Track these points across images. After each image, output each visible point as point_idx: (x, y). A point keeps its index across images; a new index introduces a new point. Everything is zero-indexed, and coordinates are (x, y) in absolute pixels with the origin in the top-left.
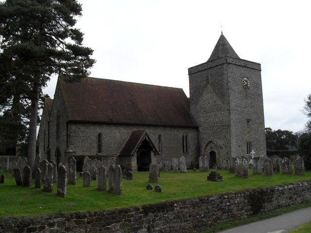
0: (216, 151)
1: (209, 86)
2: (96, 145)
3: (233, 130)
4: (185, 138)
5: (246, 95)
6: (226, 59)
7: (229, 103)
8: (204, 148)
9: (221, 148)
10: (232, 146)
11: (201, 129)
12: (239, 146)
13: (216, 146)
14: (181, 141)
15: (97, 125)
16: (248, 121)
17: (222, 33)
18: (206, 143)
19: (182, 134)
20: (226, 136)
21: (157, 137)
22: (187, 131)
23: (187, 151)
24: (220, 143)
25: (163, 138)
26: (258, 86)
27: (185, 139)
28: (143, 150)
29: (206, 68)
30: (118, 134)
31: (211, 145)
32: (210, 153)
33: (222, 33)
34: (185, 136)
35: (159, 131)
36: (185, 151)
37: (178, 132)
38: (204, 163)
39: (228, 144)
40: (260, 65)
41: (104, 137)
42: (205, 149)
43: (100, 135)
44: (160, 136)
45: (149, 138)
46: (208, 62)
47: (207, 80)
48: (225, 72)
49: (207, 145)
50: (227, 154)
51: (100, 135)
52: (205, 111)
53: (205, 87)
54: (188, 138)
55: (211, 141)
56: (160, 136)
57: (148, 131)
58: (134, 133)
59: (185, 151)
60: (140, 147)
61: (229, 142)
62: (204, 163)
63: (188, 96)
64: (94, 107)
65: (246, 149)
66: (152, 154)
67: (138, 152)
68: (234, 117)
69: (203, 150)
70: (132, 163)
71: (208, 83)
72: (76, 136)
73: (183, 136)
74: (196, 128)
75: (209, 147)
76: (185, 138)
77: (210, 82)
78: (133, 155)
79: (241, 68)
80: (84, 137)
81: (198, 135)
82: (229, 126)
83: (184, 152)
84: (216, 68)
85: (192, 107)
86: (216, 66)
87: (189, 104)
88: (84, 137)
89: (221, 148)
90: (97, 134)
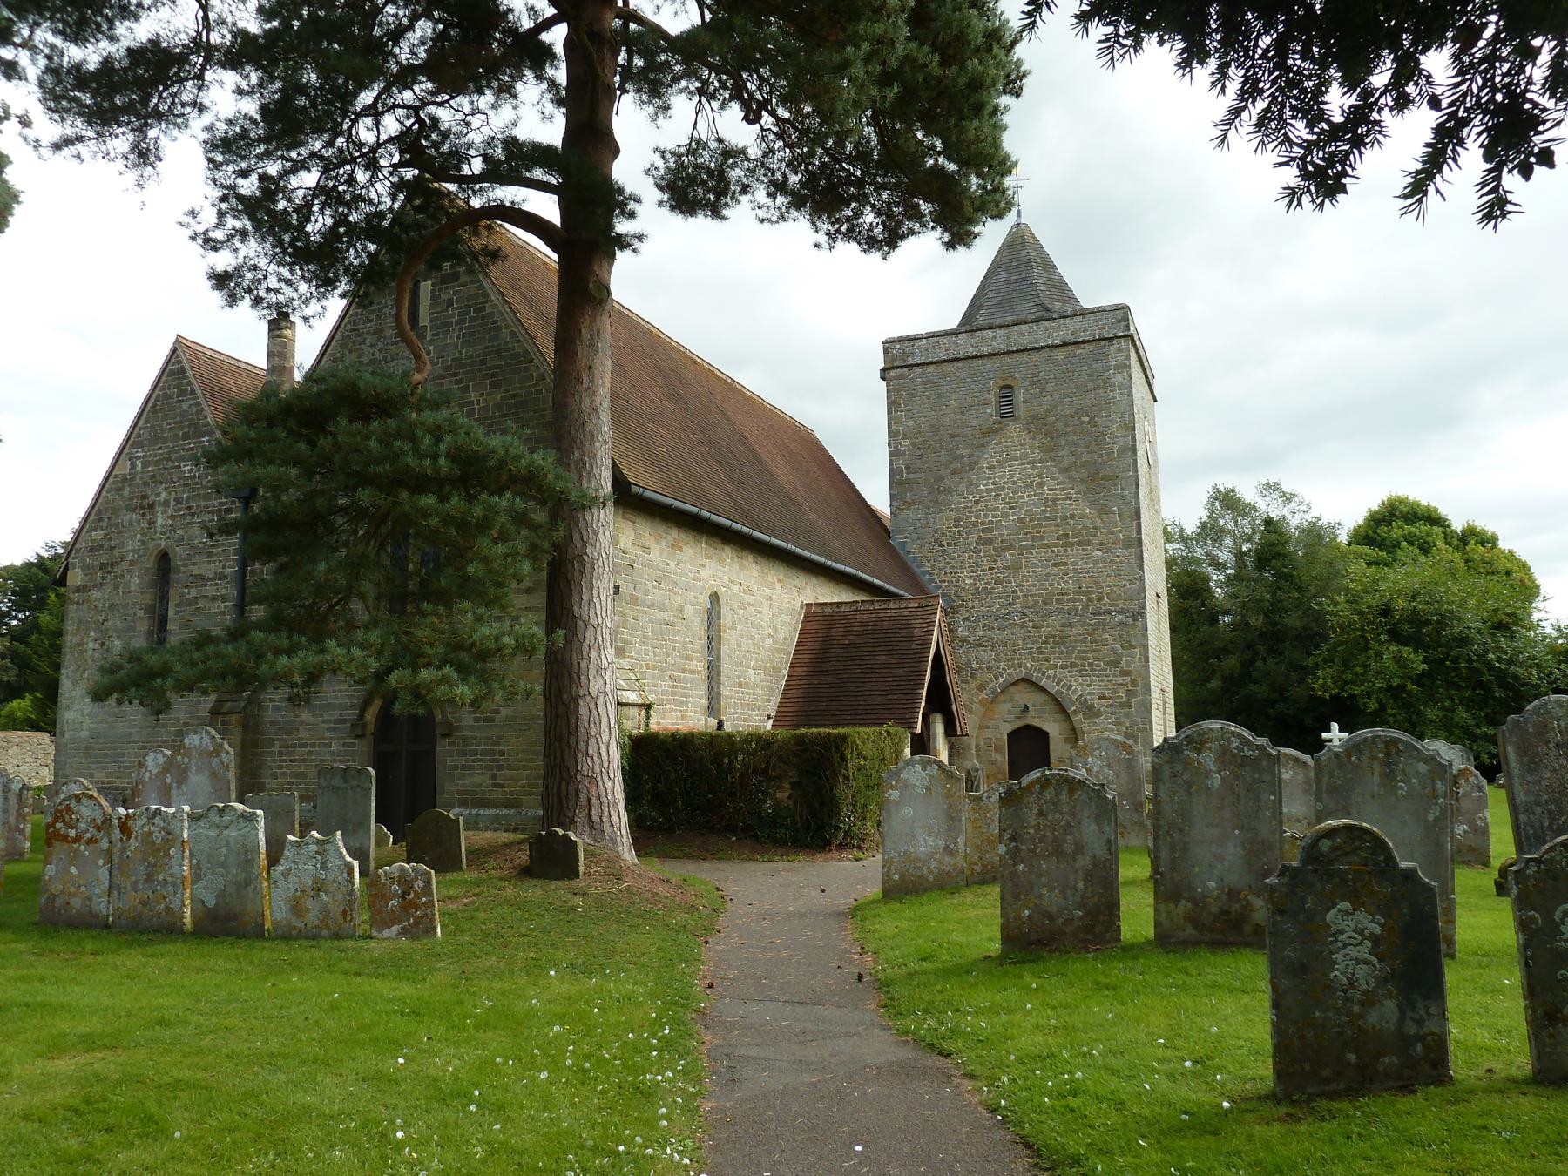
1: (1012, 425)
20: (1119, 657)
24: (1077, 687)
31: (1023, 696)
39: (1130, 693)
53: (990, 433)
75: (1004, 708)
77: (1021, 410)
84: (1060, 355)
86: (1065, 344)
89: (1091, 712)
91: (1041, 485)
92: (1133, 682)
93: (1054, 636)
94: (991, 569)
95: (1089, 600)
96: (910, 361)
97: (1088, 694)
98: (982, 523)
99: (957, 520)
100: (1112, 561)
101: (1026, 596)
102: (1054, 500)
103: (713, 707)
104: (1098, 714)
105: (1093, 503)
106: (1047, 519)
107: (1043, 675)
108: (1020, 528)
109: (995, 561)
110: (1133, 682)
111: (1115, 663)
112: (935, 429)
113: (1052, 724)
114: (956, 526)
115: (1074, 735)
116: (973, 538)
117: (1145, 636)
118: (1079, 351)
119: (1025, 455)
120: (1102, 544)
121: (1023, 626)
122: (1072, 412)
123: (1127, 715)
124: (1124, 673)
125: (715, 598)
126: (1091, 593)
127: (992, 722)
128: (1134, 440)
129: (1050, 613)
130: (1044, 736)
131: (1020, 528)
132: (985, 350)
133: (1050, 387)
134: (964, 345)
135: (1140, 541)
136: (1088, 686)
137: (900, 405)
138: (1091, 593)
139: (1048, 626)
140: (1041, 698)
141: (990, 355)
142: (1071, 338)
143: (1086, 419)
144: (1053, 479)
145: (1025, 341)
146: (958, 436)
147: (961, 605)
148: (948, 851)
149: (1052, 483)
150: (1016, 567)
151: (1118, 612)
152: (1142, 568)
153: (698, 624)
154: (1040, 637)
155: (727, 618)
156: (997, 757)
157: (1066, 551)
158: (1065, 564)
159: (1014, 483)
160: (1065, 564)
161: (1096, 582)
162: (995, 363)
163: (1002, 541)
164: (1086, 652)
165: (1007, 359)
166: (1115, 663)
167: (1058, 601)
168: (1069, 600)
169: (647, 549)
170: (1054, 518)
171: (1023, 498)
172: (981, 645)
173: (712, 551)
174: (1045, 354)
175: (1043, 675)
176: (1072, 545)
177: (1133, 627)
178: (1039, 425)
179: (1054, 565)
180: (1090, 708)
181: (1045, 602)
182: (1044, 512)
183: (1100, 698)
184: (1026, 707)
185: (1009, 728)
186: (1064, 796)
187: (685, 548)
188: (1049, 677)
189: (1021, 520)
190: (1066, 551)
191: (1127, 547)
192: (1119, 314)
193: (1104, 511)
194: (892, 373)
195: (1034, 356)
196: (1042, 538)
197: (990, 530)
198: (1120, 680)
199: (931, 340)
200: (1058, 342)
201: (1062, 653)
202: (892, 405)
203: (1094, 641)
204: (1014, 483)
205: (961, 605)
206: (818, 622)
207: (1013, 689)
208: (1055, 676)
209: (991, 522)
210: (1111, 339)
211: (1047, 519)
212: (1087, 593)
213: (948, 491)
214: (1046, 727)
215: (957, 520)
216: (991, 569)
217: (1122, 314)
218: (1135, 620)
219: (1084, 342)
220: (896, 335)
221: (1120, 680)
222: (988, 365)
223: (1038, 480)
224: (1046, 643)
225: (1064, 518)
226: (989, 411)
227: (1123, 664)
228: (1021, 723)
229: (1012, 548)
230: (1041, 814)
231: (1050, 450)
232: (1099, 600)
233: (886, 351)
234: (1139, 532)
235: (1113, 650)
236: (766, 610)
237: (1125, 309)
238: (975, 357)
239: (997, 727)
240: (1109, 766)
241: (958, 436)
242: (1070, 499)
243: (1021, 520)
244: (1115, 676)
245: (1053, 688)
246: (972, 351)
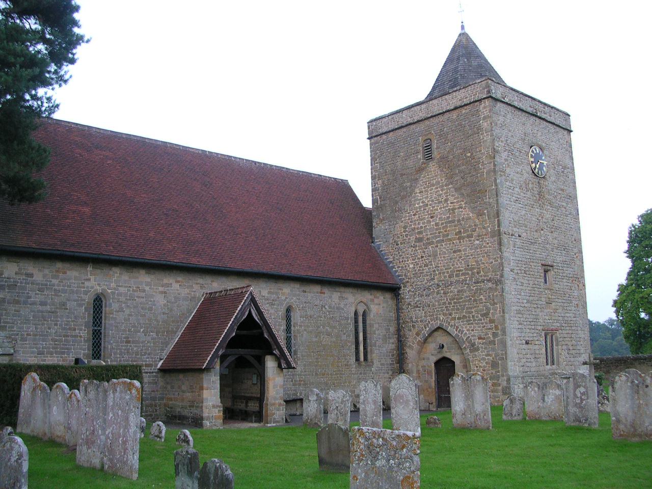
1: (431, 164)
2: (85, 333)
3: (510, 287)
4: (360, 319)
5: (540, 193)
6: (488, 86)
7: (498, 214)
8: (415, 346)
9: (474, 348)
10: (509, 343)
11: (405, 292)
12: (527, 343)
13: (457, 342)
14: (352, 327)
15: (90, 268)
16: (547, 269)
17: (463, 27)
18: (426, 332)
19: (354, 310)
20: (488, 309)
21: (282, 312)
22: (366, 296)
23: (366, 359)
24: (468, 331)
25: (296, 317)
26: (567, 171)
27: (361, 320)
28: (242, 351)
29: (422, 115)
30: (161, 300)
31: (440, 338)
32: (437, 363)
33: (463, 27)
34: (361, 312)
35: (288, 293)
36: (362, 358)
37: (341, 298)
38: (469, 396)
39: (495, 335)
40: (569, 116)
41: (111, 308)
42: (419, 352)
43: (98, 304)
44: (288, 310)
45: (260, 313)
46: (431, 97)
48: (485, 125)
49: (426, 340)
50: (494, 365)
51: (98, 304)
53: (420, 170)
54: (371, 317)
55: (439, 328)
56: (288, 310)
57: (262, 291)
58: (211, 300)
59: (362, 358)
60: (233, 343)
61: (499, 329)
62: (469, 396)
63: (367, 201)
64: (87, 210)
65: (544, 350)
66: (270, 364)
67: (223, 358)
68: (512, 254)
69: (411, 354)
70: (206, 394)
72: (18, 302)
73: (356, 313)
74: (393, 290)
75: (432, 347)
76: (360, 319)
77: (435, 154)
78: (208, 369)
79: (523, 117)
80: (43, 304)
81: (398, 310)
82: (499, 282)
83: (357, 359)
84: (454, 115)
85: (379, 229)
86: (456, 108)
87: (372, 223)
88: (43, 304)
89: (474, 348)
90: (88, 299)
91: (446, 200)
92: (496, 327)
93: (454, 299)
94: (422, 257)
95: (473, 274)
96: (381, 131)
97: (472, 336)
98: (418, 228)
99: (405, 227)
100: (484, 247)
101: (440, 273)
102: (453, 209)
104: (477, 349)
105: (473, 209)
106: (450, 222)
107: (449, 324)
108: (437, 229)
109: (424, 252)
110: (496, 327)
111: (486, 315)
112: (393, 173)
113: (456, 356)
114: (404, 232)
116: (413, 238)
118: (464, 112)
119: (438, 183)
120: (479, 236)
121: (438, 293)
122: (461, 151)
123: (493, 349)
124: (491, 321)
126: (474, 269)
127: (426, 356)
129: (451, 284)
130: (453, 363)
131: (437, 229)
136: (473, 330)
137: (376, 160)
138: (474, 269)
139: (451, 292)
140: (450, 339)
142: (459, 104)
143: (469, 154)
144: (453, 196)
145: (436, 110)
146: (404, 174)
147: (408, 282)
149: (451, 199)
150: (435, 256)
151: (488, 281)
154: (447, 300)
157: (460, 242)
158: (460, 251)
159: (433, 201)
160: (460, 251)
161: (477, 262)
163: (428, 239)
164: (471, 308)
165: (427, 122)
166: (486, 315)
167: (457, 275)
168: (463, 274)
169: (31, 275)
170: (453, 221)
171: (437, 210)
172: (417, 307)
174: (447, 116)
175: (449, 324)
177: (496, 290)
178: (444, 161)
179: (455, 252)
180: (473, 345)
181: (450, 277)
182: (448, 218)
183: (479, 338)
184: (443, 346)
185: (434, 359)
187: (69, 273)
188: (452, 326)
189: (437, 224)
190: (460, 242)
191: (493, 237)
193: (480, 214)
195: (441, 118)
196: (448, 235)
198: (489, 326)
199: (390, 117)
200: (452, 108)
201: (458, 309)
203: (475, 300)
204: (433, 201)
205: (408, 282)
207: (436, 334)
208: (455, 325)
209: (422, 227)
210: (480, 101)
211: (450, 222)
212: (472, 269)
213: (400, 210)
215: (405, 227)
216: (422, 257)
219: (465, 105)
221: (489, 326)
223: (445, 198)
224: (450, 303)
225: (459, 221)
226: (419, 157)
227: (490, 315)
228: (440, 356)
229: (432, 243)
231: (450, 178)
232: (478, 273)
233: (369, 128)
235: (485, 306)
238: (410, 124)
239: (428, 359)
241: (404, 174)
242: (461, 208)
243: (437, 224)
244: (486, 323)
245: (454, 332)
246: (410, 120)
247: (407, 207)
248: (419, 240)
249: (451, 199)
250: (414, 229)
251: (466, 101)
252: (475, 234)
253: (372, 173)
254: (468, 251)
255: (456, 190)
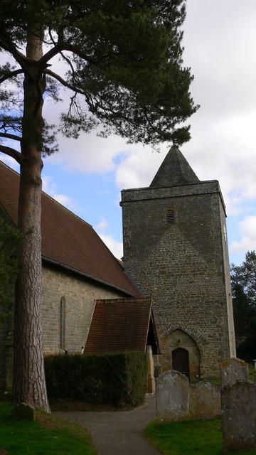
0: (190, 350)
1: (174, 228)
13: (192, 340)
24: (200, 333)
31: (178, 336)
47: (171, 219)
50: (220, 353)
52: (163, 273)
53: (164, 229)
71: (171, 219)
77: (177, 220)
84: (192, 199)
86: (194, 195)
89: (205, 342)
92: (222, 330)
99: (151, 264)
103: (62, 346)
110: (222, 330)
111: (215, 323)
115: (198, 352)
116: (157, 271)
117: (226, 311)
125: (63, 298)
128: (221, 233)
130: (187, 352)
132: (162, 196)
133: (188, 211)
134: (154, 194)
135: (224, 272)
140: (185, 337)
141: (164, 198)
148: (183, 409)
150: (175, 283)
152: (224, 284)
153: (57, 309)
155: (68, 306)
156: (167, 361)
161: (206, 290)
162: (166, 202)
166: (215, 323)
173: (62, 279)
176: (197, 275)
181: (186, 297)
183: (210, 336)
184: (179, 340)
185: (172, 349)
186: (246, 390)
192: (214, 184)
193: (209, 261)
194: (125, 204)
195: (181, 199)
197: (164, 268)
200: (191, 194)
202: (124, 217)
206: (101, 306)
209: (165, 265)
212: (203, 294)
214: (187, 349)
217: (215, 184)
218: (222, 305)
220: (126, 189)
222: (163, 202)
228: (177, 347)
230: (237, 397)
234: (223, 270)
236: (81, 303)
237: (216, 182)
240: (235, 371)
245: (190, 333)
247: (153, 251)
248: (163, 273)
249: (188, 250)
250: (158, 266)
251: (200, 192)
252: (206, 273)
253: (123, 225)
254: (201, 283)
255: (192, 245)
